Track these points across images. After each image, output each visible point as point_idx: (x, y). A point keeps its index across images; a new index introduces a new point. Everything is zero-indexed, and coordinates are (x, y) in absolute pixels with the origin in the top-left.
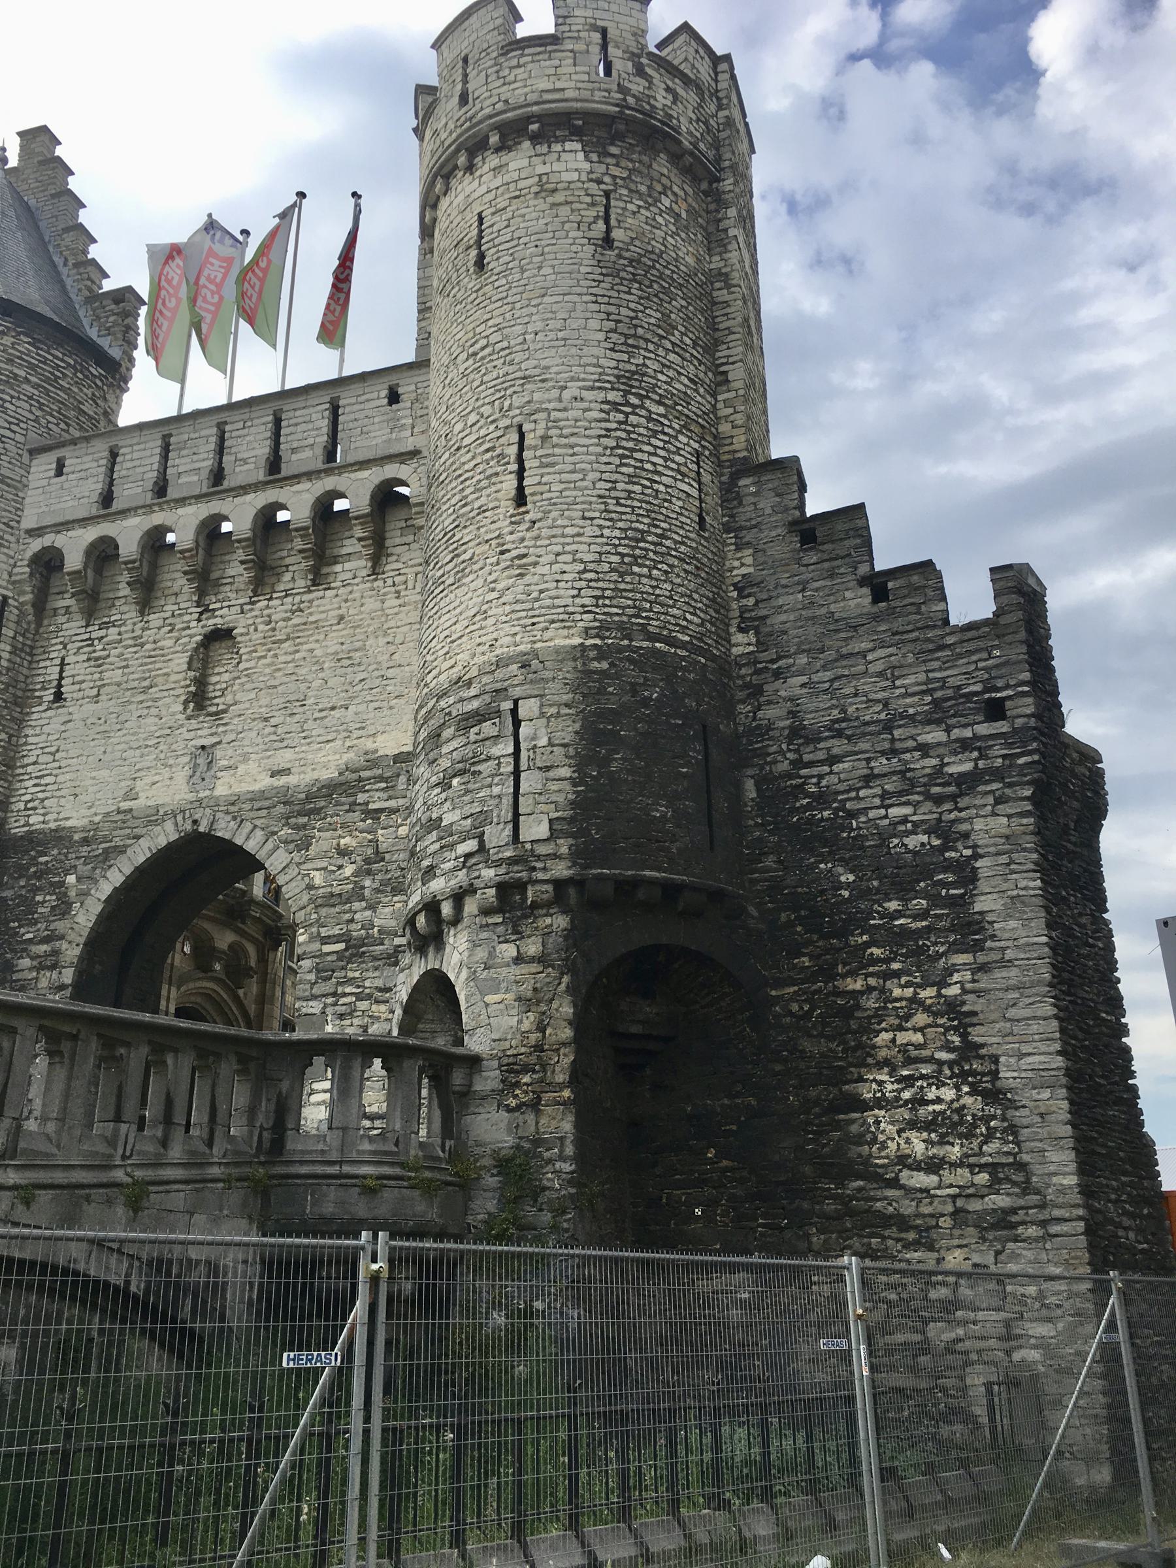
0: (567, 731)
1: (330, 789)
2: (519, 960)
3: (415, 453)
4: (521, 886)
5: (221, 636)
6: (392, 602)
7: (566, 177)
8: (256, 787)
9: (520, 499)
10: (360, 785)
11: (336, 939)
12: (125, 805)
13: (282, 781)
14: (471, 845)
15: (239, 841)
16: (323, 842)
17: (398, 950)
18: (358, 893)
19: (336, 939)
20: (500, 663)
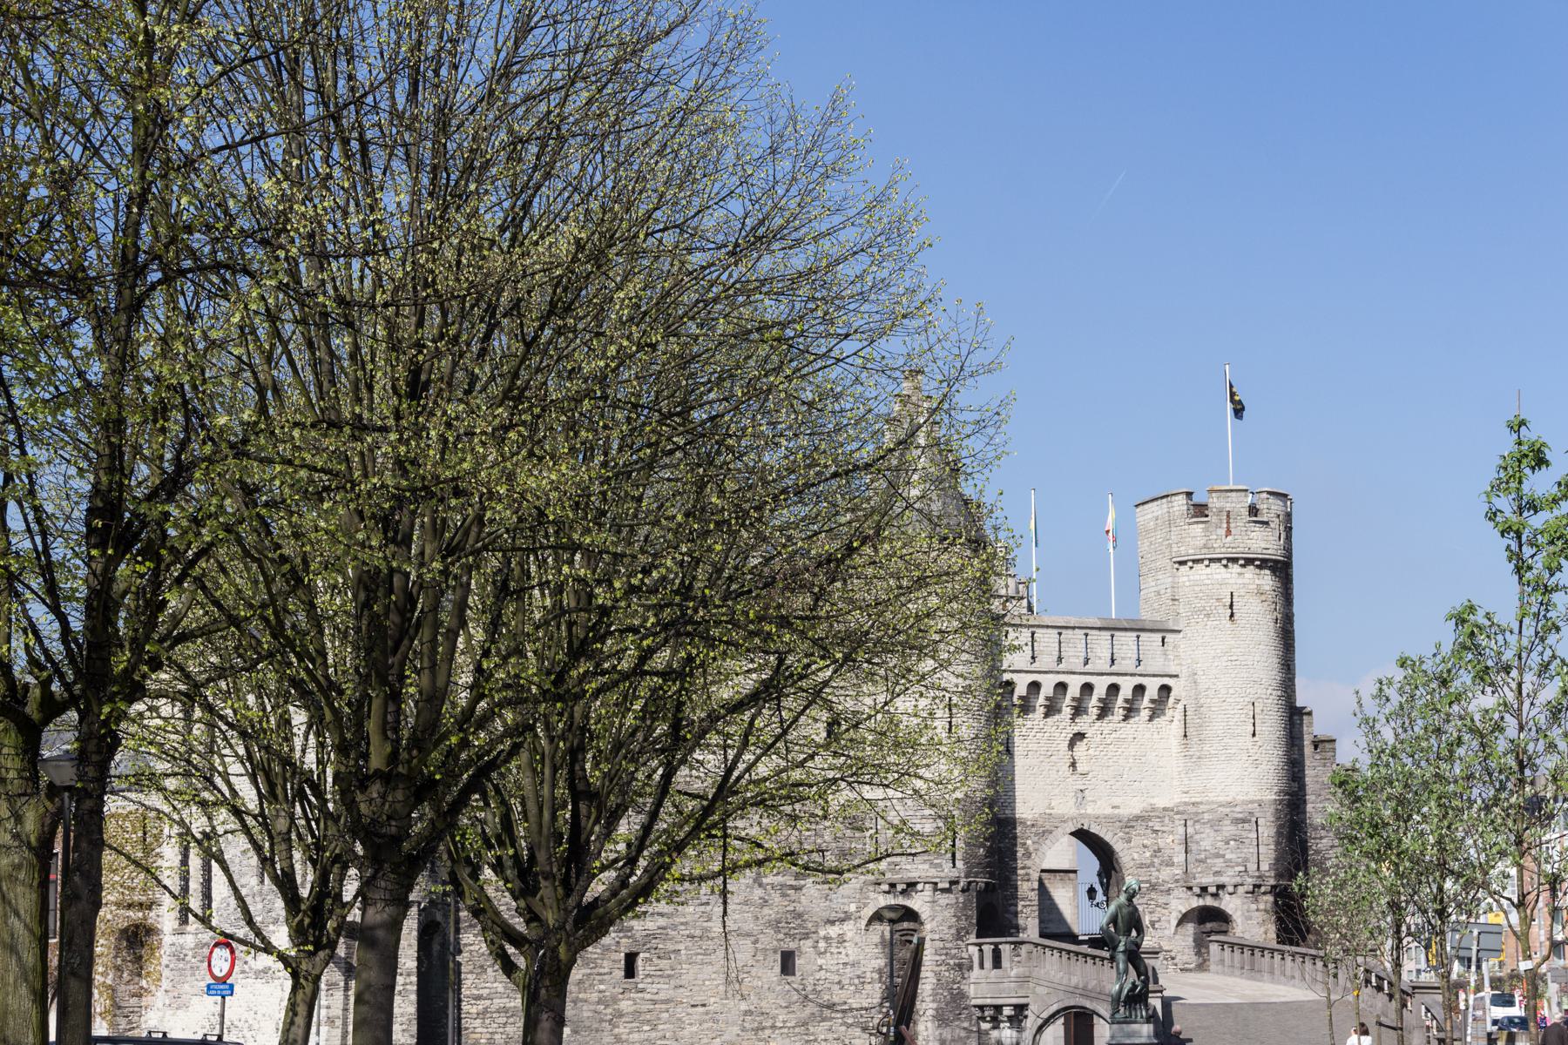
0: (1272, 831)
1: (1137, 818)
2: (1258, 910)
3: (1177, 676)
4: (1259, 886)
5: (1080, 736)
6: (1156, 736)
7: (1268, 588)
8: (1106, 812)
9: (1254, 735)
10: (1149, 819)
11: (1147, 882)
12: (1048, 811)
13: (1116, 811)
14: (1243, 869)
15: (1102, 835)
16: (1136, 841)
17: (1169, 889)
18: (1152, 864)
19: (1147, 882)
20: (1252, 802)
